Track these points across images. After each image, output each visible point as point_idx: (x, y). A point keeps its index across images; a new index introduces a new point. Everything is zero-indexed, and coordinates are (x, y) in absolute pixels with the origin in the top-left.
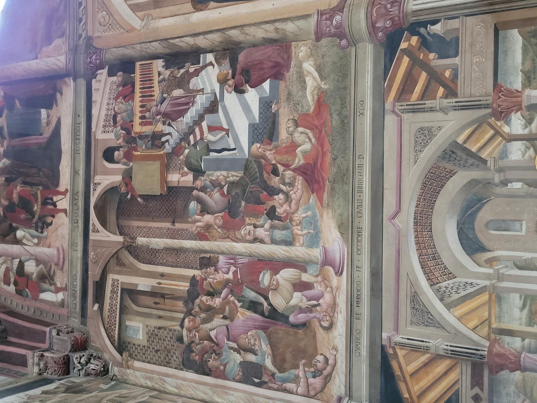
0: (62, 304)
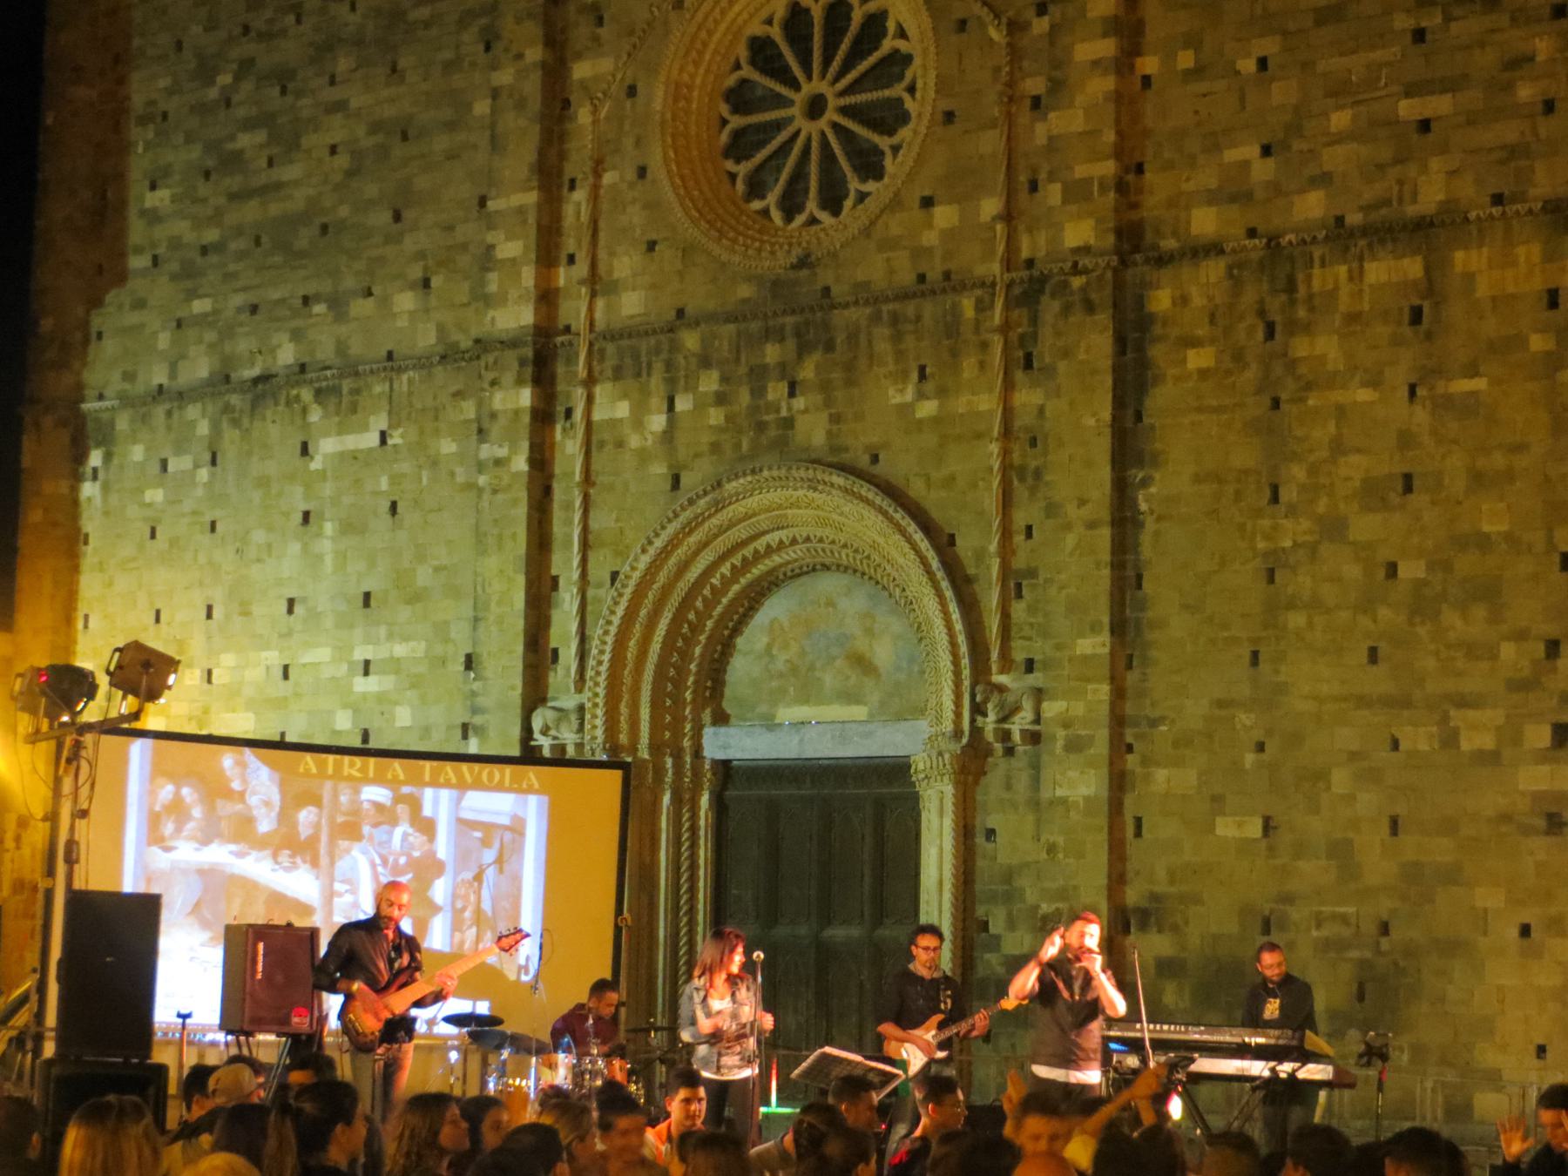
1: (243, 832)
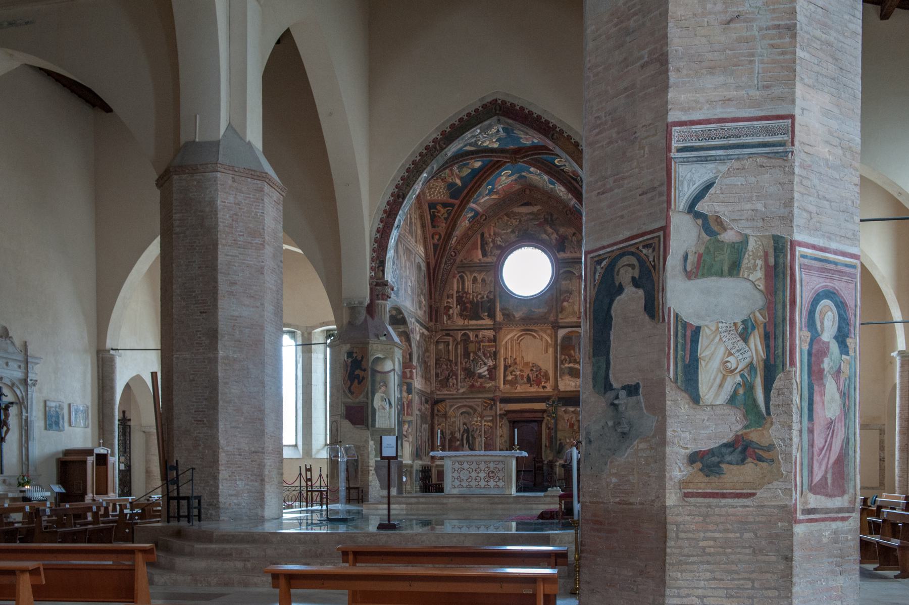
0: (444, 323)
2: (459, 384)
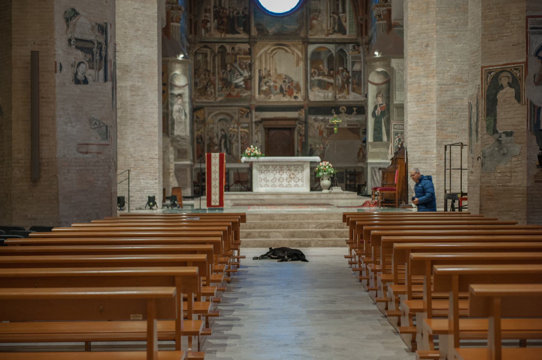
0: (202, 36)
1: (324, 75)
2: (217, 93)
